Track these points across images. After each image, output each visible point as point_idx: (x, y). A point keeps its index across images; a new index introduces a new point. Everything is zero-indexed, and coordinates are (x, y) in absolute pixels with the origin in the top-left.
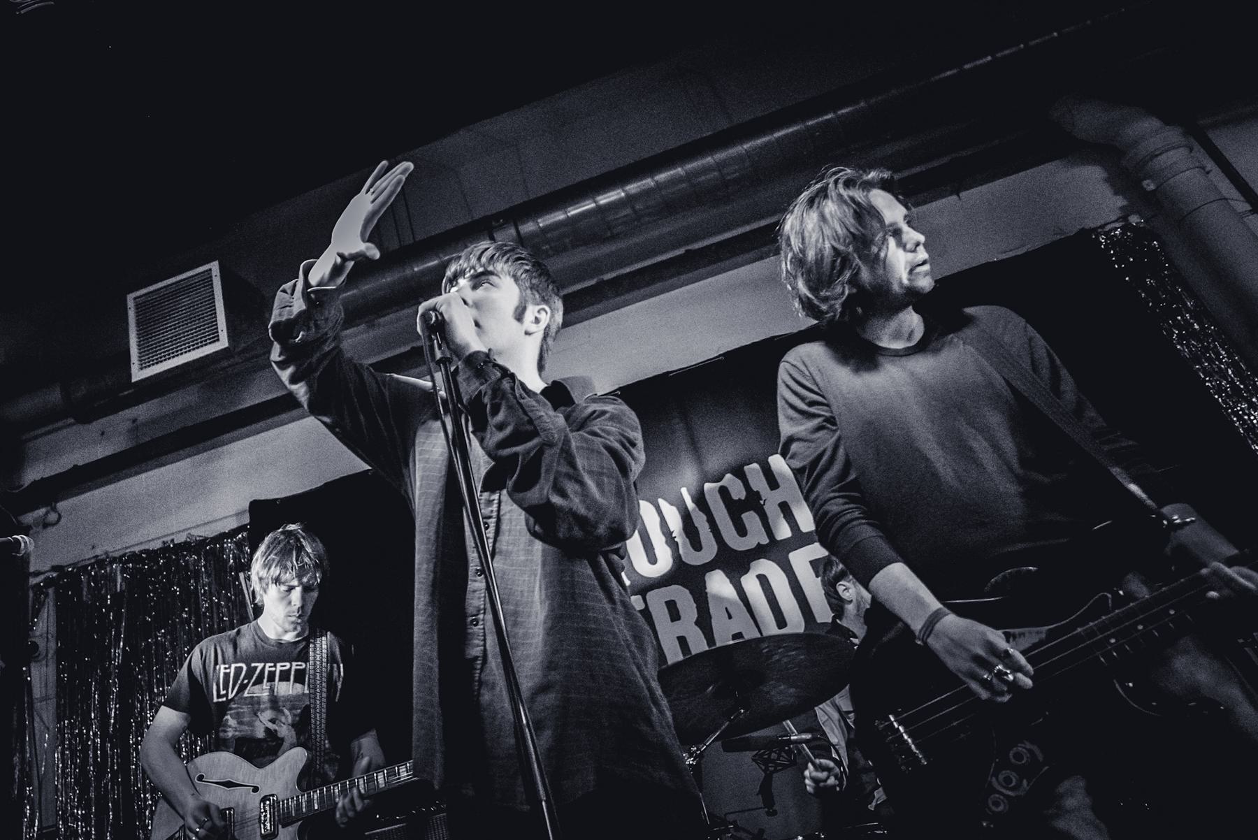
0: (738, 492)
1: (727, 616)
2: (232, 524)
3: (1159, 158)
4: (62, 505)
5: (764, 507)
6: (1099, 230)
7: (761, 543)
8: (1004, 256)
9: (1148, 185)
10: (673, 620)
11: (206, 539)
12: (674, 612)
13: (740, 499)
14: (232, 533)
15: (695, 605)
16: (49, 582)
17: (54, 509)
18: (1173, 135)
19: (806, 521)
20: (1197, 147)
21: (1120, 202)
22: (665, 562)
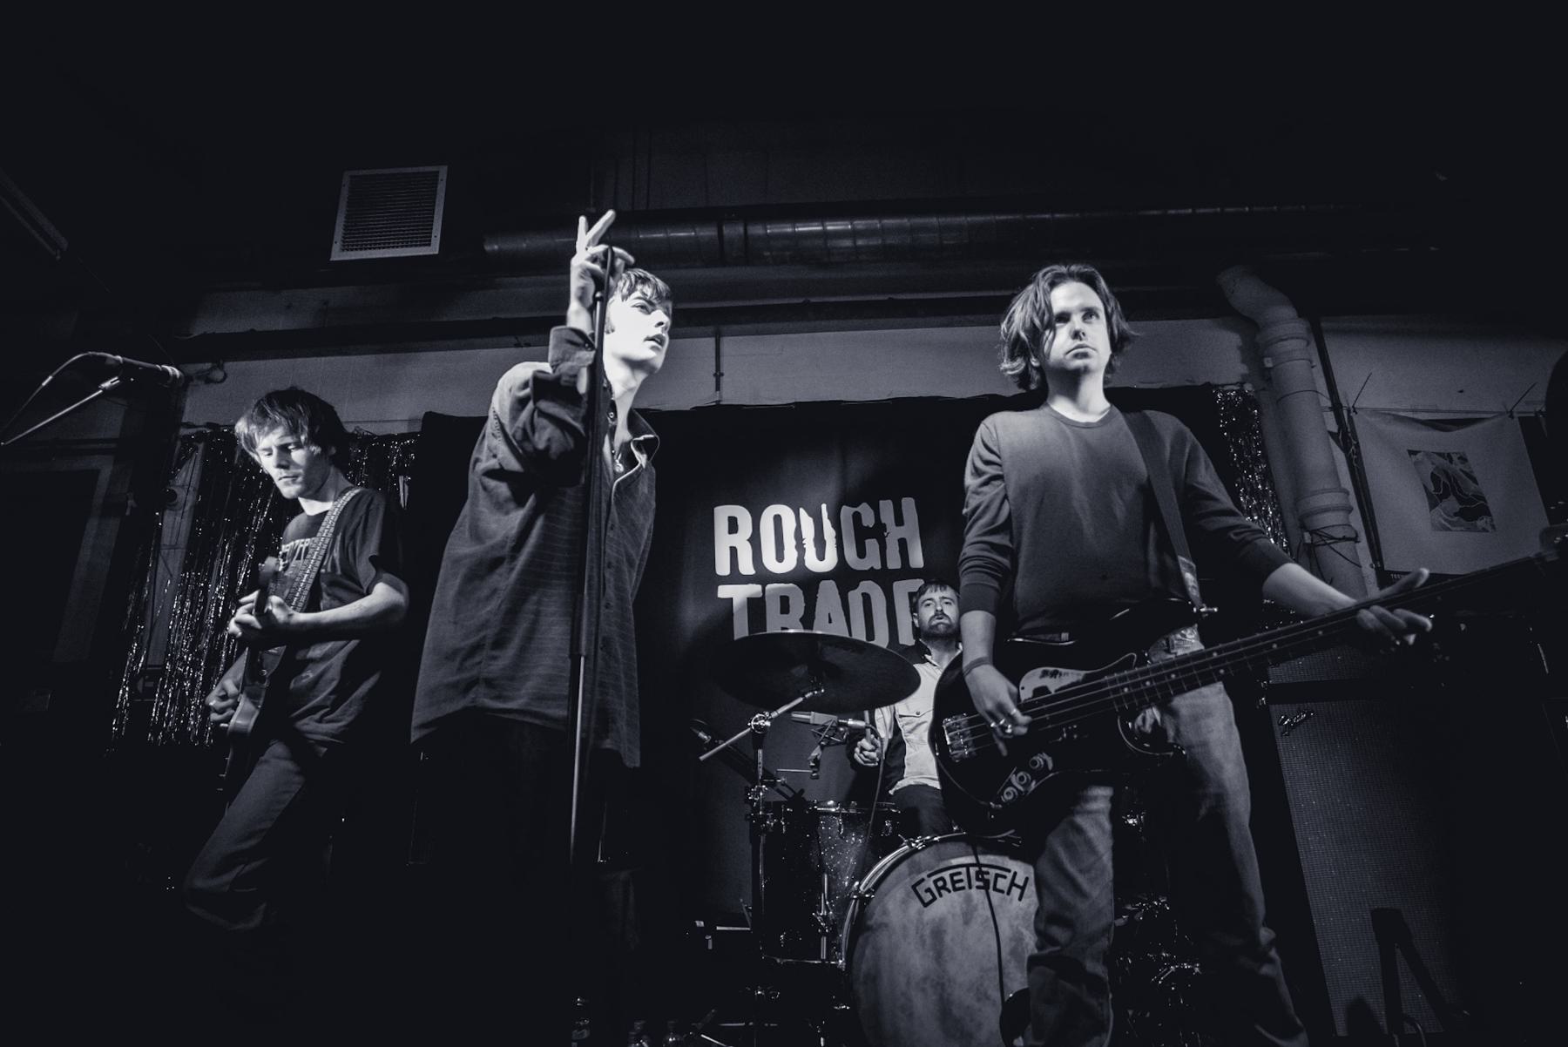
0: (868, 520)
1: (828, 620)
2: (403, 429)
3: (1285, 343)
4: (230, 366)
5: (887, 539)
6: (1220, 388)
7: (875, 567)
8: (1142, 386)
9: (1268, 362)
10: (782, 613)
11: (374, 436)
12: (785, 605)
13: (868, 527)
14: (402, 437)
15: (804, 605)
16: (201, 437)
17: (221, 367)
18: (1300, 327)
19: (917, 559)
20: (1313, 344)
21: (1243, 369)
22: (789, 564)
